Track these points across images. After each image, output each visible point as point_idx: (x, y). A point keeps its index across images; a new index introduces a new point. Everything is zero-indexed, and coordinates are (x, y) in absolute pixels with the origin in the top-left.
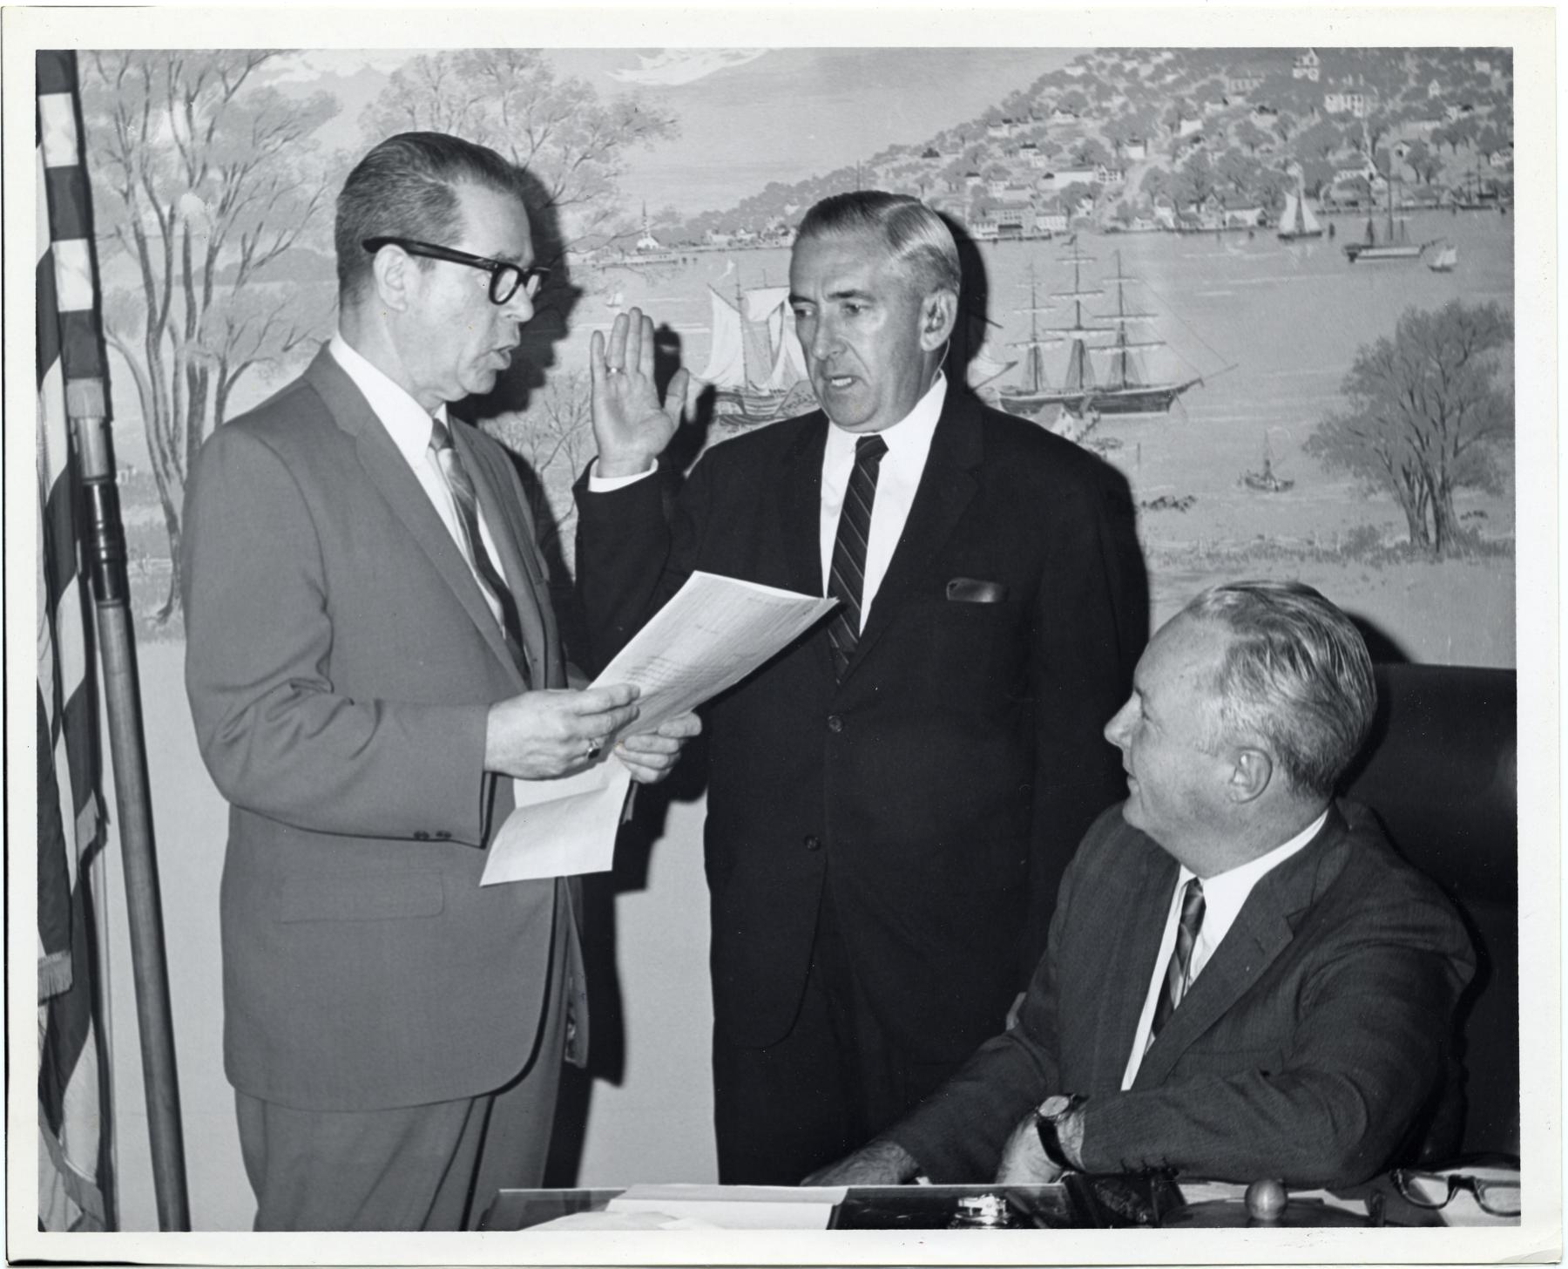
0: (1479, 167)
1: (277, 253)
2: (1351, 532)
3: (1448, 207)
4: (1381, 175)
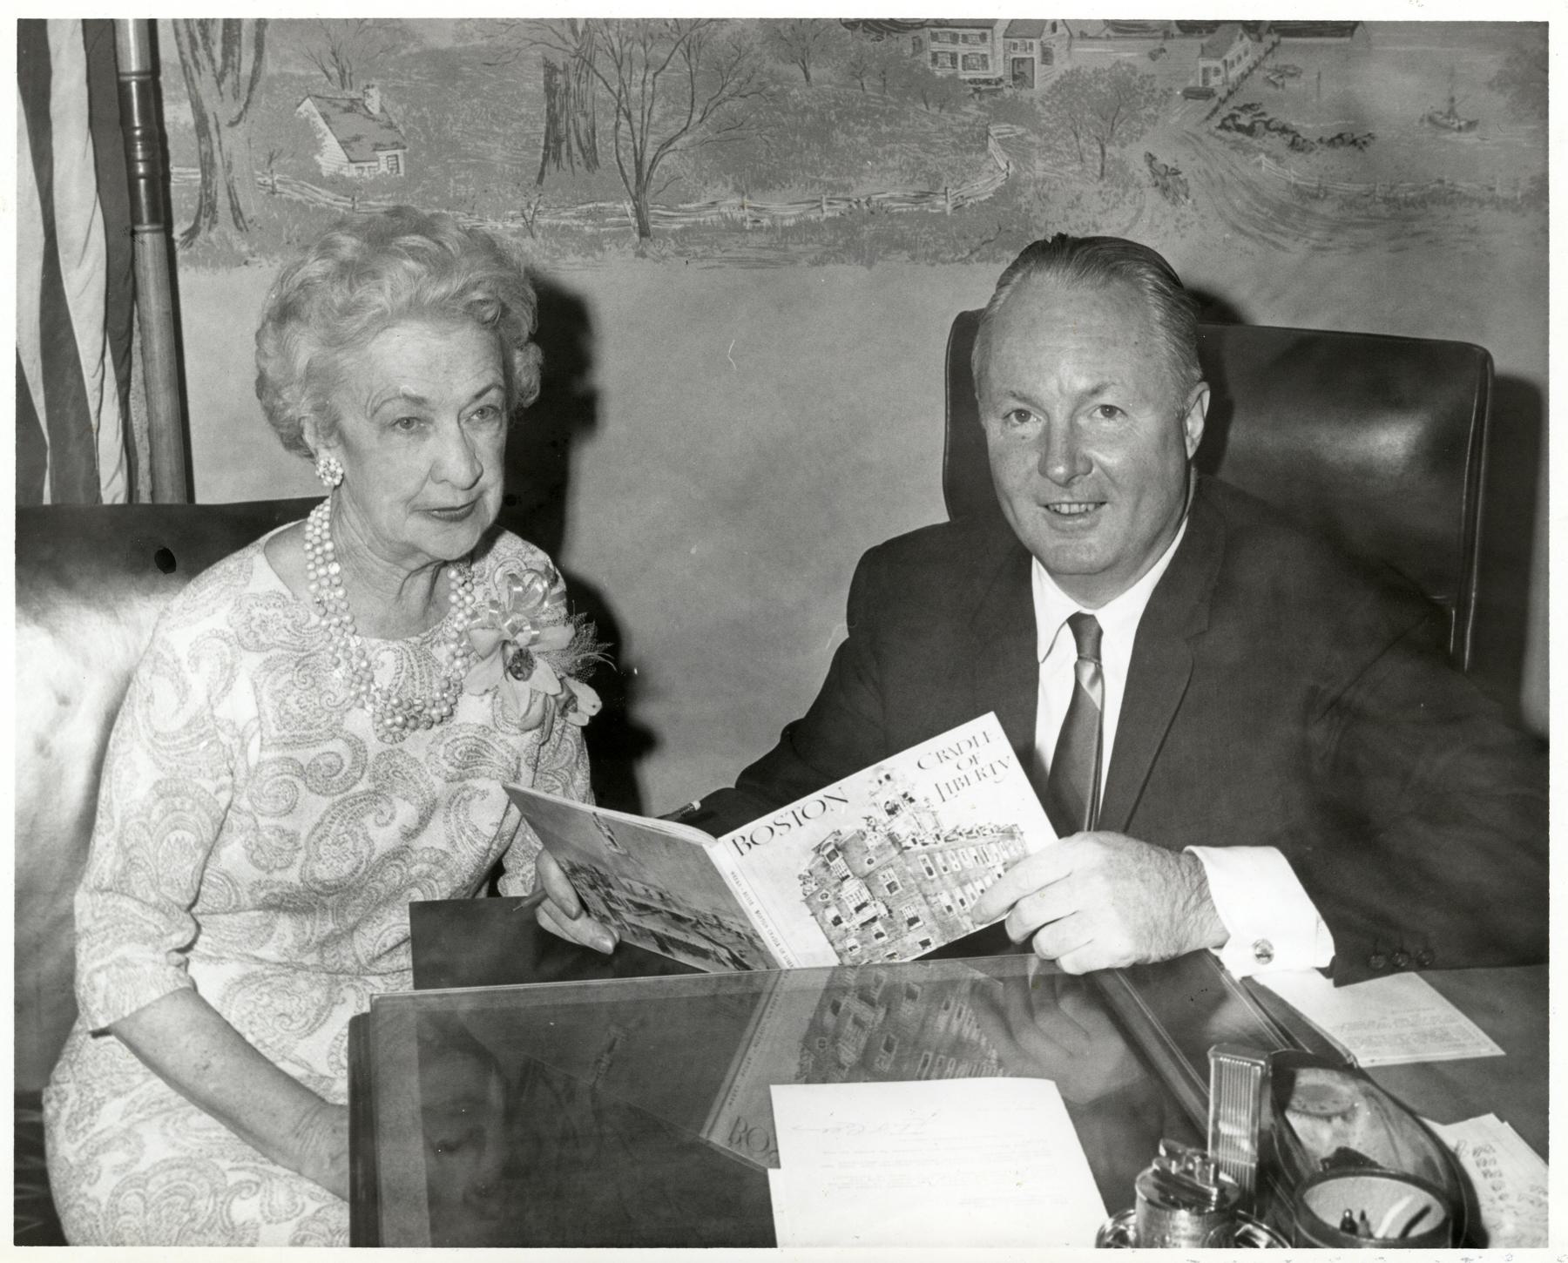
2: (1532, 178)
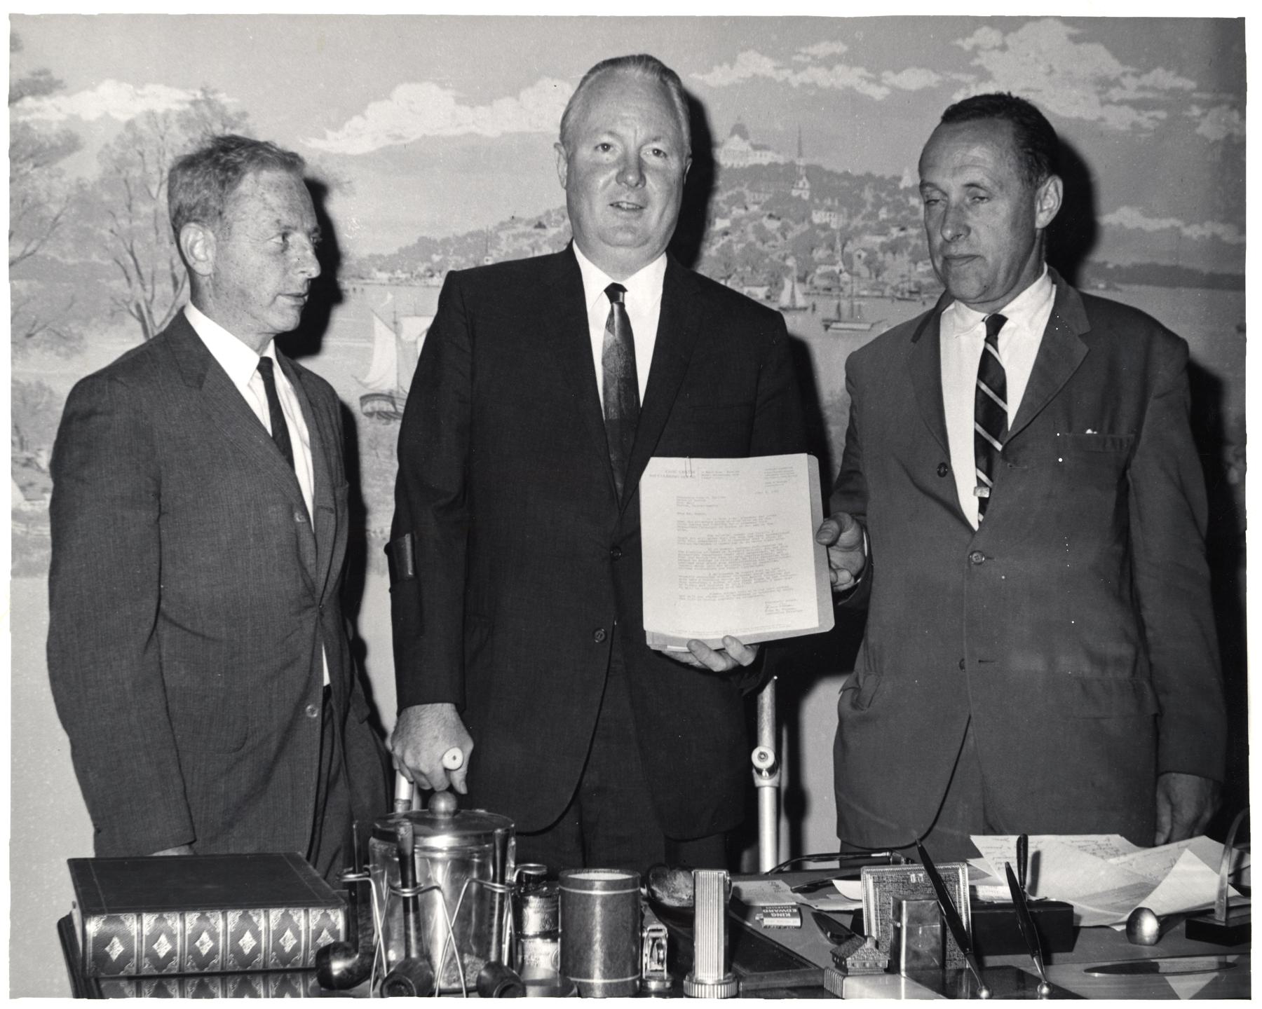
0: (910, 271)
1: (25, 257)
3: (889, 297)
4: (846, 271)
